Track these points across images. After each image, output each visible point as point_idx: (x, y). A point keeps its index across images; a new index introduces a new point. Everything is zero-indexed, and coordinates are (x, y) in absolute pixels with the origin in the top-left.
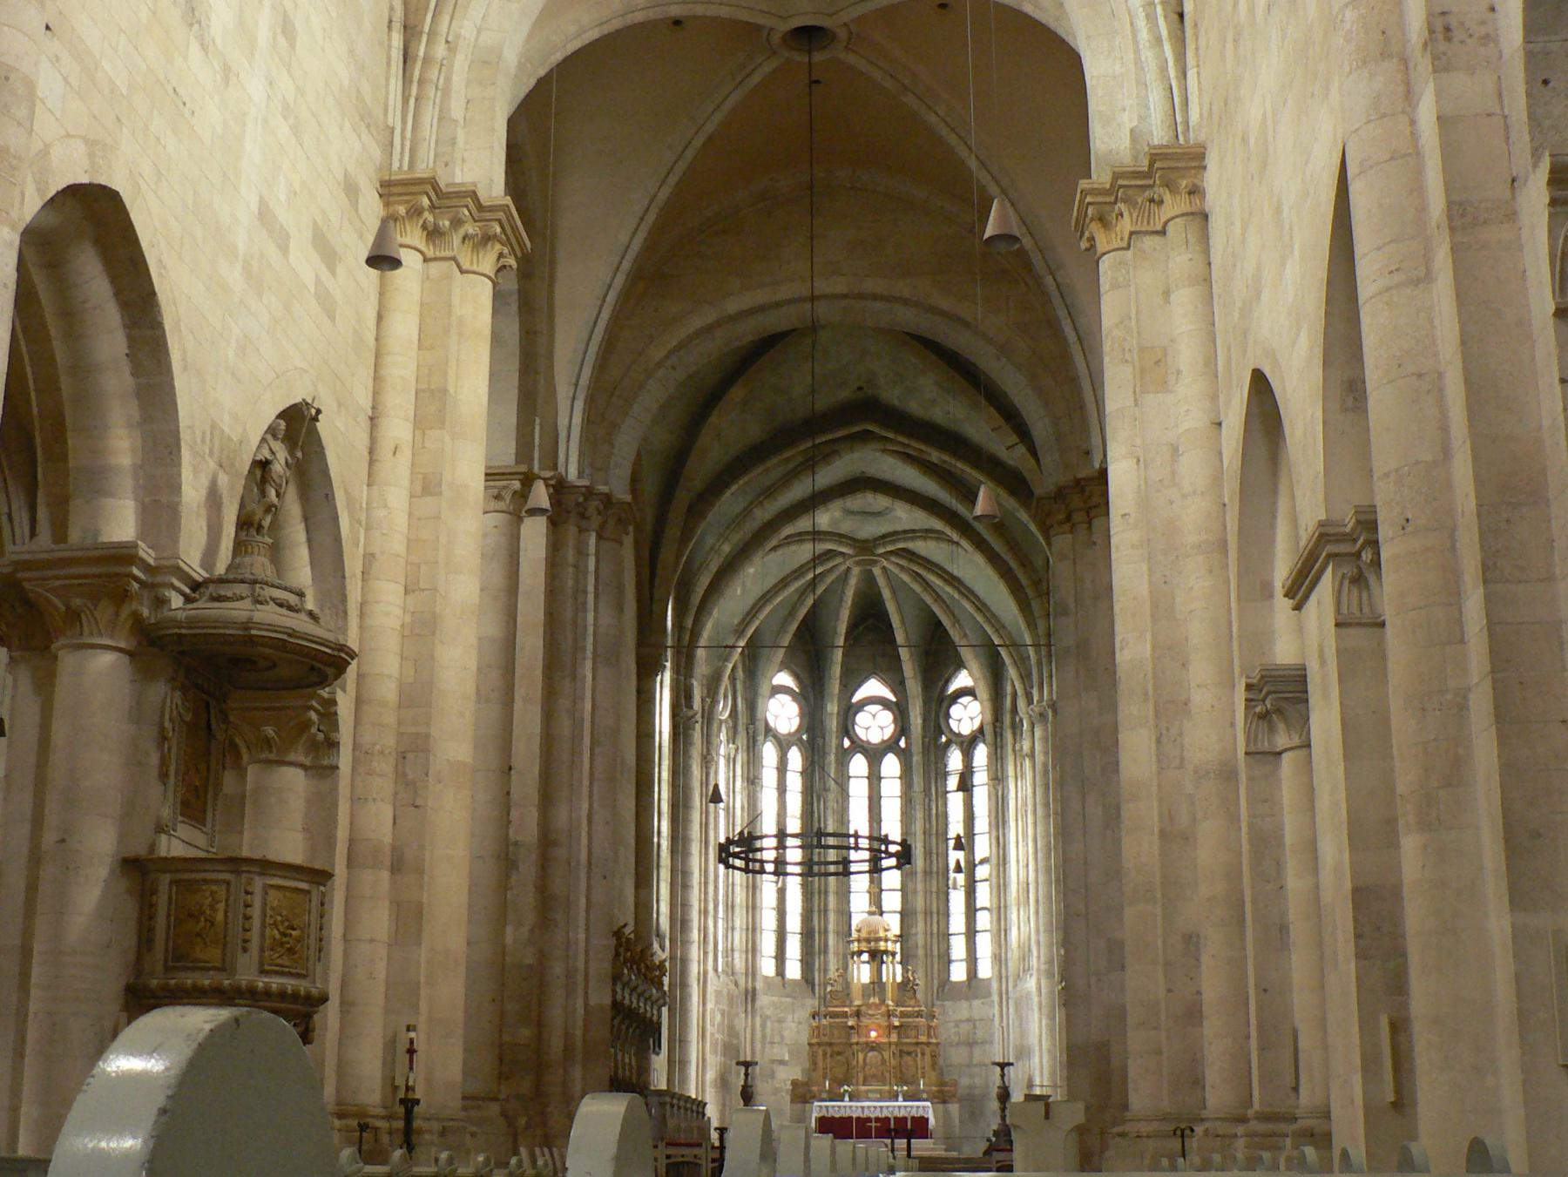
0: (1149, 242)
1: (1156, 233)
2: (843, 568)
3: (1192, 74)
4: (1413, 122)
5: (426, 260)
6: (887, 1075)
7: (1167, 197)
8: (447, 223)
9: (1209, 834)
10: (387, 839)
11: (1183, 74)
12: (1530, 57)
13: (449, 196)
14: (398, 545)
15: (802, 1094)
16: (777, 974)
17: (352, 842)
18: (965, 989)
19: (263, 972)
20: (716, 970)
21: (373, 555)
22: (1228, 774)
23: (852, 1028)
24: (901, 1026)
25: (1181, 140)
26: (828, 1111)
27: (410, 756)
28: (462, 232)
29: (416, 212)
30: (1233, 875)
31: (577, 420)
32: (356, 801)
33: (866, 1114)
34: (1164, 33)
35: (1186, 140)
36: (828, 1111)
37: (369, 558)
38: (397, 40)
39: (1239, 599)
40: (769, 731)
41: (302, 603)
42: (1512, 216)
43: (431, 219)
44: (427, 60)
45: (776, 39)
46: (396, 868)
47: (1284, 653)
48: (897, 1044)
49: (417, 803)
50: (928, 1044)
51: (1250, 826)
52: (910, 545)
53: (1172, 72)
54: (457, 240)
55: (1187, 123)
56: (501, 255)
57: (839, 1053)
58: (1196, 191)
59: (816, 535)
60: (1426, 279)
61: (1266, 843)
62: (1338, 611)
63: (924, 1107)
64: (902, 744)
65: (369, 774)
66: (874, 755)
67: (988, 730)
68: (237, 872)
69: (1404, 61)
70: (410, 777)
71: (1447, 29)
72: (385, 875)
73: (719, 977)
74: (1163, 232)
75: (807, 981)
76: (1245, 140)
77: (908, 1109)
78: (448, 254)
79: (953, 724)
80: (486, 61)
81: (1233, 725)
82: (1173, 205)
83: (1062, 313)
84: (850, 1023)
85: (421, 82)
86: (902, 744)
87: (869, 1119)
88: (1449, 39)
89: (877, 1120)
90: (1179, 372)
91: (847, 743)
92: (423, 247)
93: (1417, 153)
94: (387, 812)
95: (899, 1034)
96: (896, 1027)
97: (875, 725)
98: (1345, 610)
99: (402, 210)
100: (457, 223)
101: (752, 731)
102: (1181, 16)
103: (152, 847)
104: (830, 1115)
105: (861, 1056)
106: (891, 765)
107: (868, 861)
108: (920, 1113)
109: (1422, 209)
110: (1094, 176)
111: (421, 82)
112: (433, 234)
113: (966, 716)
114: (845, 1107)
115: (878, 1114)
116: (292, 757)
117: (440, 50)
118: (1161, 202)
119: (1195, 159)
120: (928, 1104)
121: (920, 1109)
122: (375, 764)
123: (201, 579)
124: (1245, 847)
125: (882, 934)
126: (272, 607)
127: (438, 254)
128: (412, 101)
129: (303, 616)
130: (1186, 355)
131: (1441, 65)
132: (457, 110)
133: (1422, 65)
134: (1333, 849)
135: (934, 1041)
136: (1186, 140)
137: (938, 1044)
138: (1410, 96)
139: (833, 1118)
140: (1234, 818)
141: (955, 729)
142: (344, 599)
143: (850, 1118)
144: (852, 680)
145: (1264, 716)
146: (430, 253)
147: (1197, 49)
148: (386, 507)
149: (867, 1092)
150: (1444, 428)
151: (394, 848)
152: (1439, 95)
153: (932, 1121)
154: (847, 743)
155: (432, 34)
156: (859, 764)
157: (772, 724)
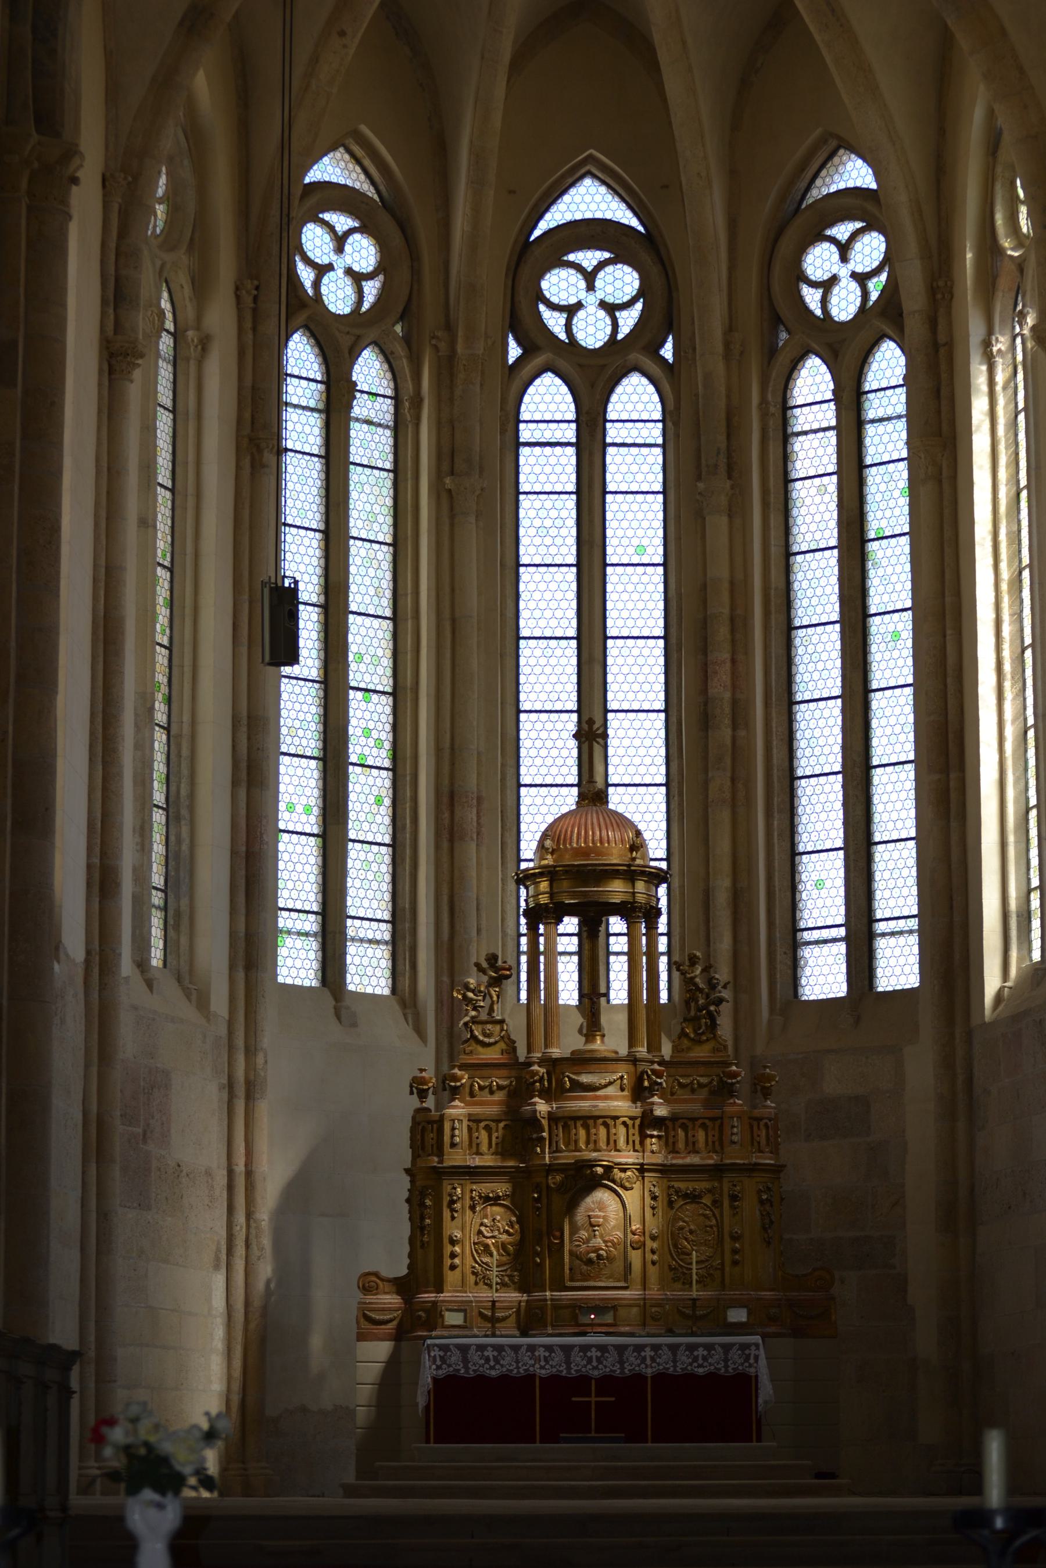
16: (324, 980)
20: (142, 963)
24: (674, 1118)
26: (465, 1361)
33: (578, 1364)
36: (465, 1361)
50: (752, 1169)
63: (744, 1347)
64: (667, 352)
67: (914, 301)
73: (150, 984)
75: (403, 1004)
77: (701, 1352)
79: (812, 298)
86: (667, 352)
87: (581, 1383)
89: (607, 1383)
91: (514, 351)
96: (659, 1123)
104: (472, 1374)
108: (736, 1363)
114: (516, 1348)
115: (610, 1365)
120: (758, 1339)
121: (735, 1355)
125: (616, 856)
137: (777, 1170)
139: (481, 1378)
143: (530, 1378)
153: (766, 1390)
154: (514, 351)
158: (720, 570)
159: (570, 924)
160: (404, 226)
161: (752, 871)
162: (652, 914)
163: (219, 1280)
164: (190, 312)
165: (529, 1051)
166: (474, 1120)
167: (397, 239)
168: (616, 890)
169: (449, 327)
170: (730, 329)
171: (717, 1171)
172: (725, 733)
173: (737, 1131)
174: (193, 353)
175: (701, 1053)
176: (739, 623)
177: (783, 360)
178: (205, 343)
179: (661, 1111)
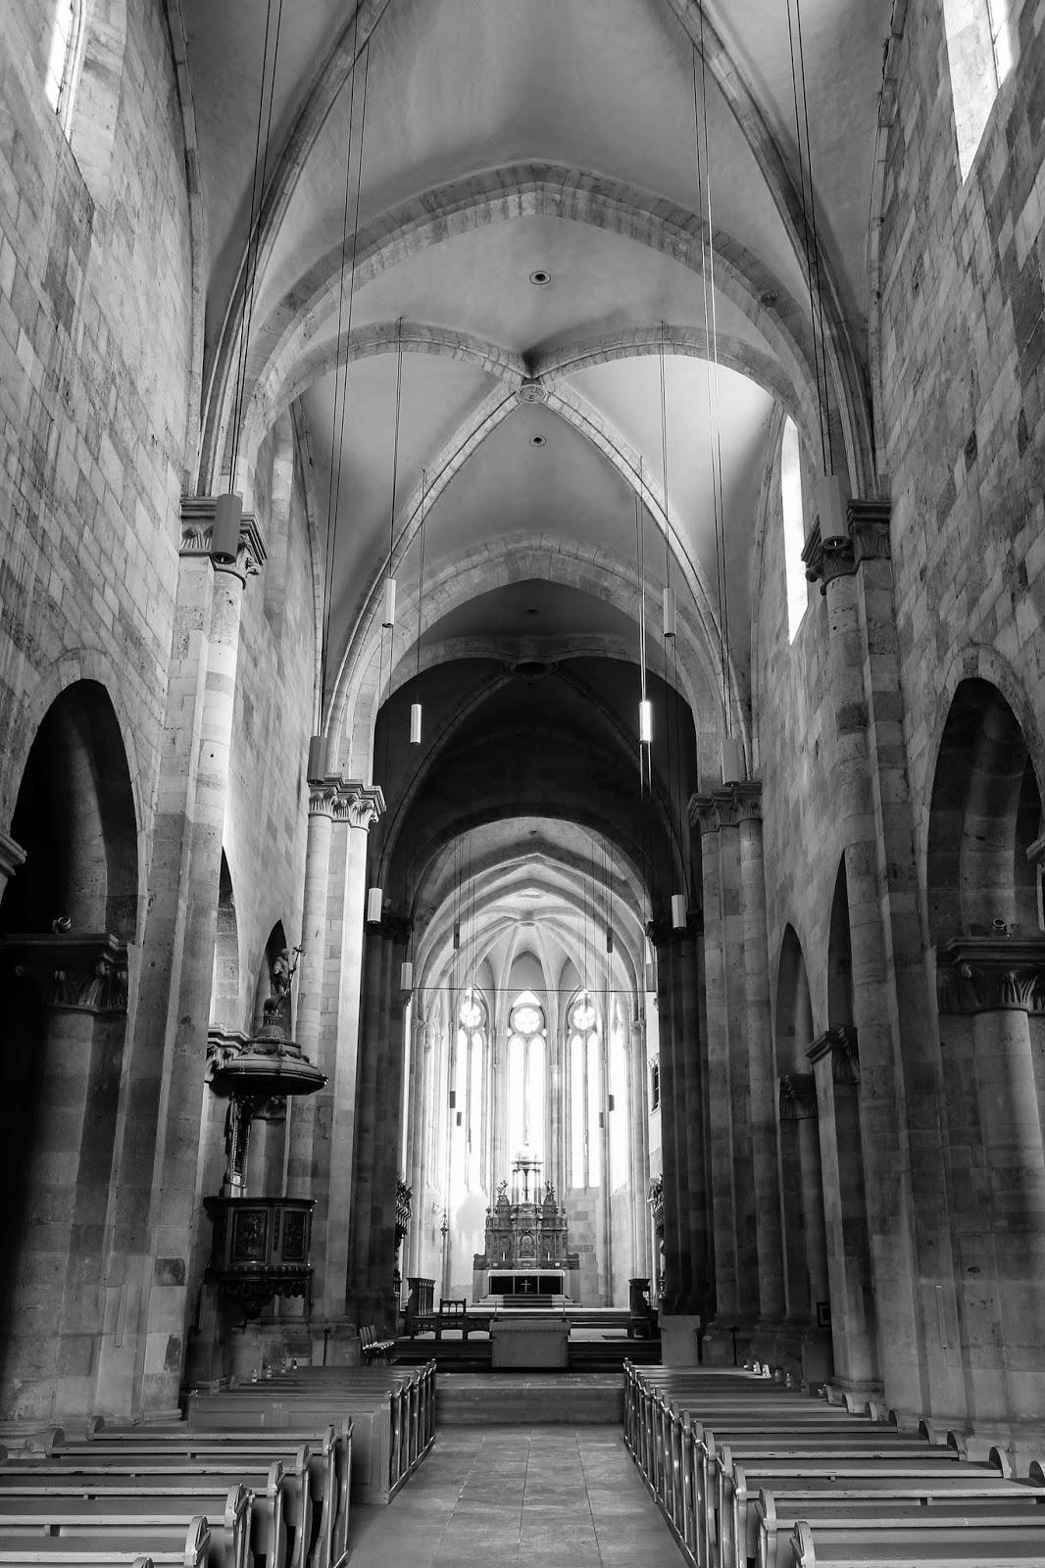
0: (729, 831)
1: (734, 826)
2: (514, 927)
3: (755, 741)
4: (879, 907)
5: (333, 822)
6: (535, 1251)
7: (741, 809)
8: (346, 802)
9: (759, 1161)
10: (310, 1159)
11: (750, 740)
12: (930, 896)
13: (346, 786)
14: (318, 988)
15: (480, 1264)
17: (290, 1161)
18: (583, 1193)
19: (284, 1260)
21: (304, 994)
22: (769, 1128)
23: (513, 1220)
25: (749, 779)
27: (322, 1109)
28: (353, 805)
29: (328, 796)
30: (773, 1183)
31: (384, 872)
32: (294, 1137)
34: (741, 716)
35: (752, 778)
37: (302, 995)
38: (318, 693)
39: (777, 1034)
40: (461, 1025)
41: (300, 1052)
42: (921, 961)
43: (337, 799)
44: (336, 707)
45: (513, 667)
46: (314, 1174)
47: (801, 1065)
48: (542, 1231)
49: (327, 1136)
50: (561, 1230)
51: (783, 1161)
52: (556, 916)
53: (744, 739)
54: (350, 810)
55: (751, 767)
56: (372, 816)
57: (505, 1237)
58: (756, 806)
59: (499, 909)
60: (883, 981)
61: (792, 1168)
62: (834, 1077)
65: (301, 1121)
66: (527, 1039)
68: (273, 1206)
69: (876, 878)
70: (322, 1121)
71: (895, 872)
72: (308, 1179)
74: (737, 826)
76: (786, 801)
78: (345, 818)
80: (364, 703)
81: (773, 1101)
82: (742, 815)
83: (665, 822)
84: (512, 1217)
85: (332, 719)
88: (895, 877)
90: (745, 906)
92: (331, 814)
93: (881, 922)
94: (310, 1142)
95: (542, 1224)
97: (527, 1020)
98: (838, 1076)
99: (321, 795)
100: (350, 802)
101: (455, 1024)
102: (750, 706)
103: (222, 1191)
105: (519, 1239)
106: (538, 1045)
107: (587, 1187)
109: (883, 953)
110: (700, 790)
111: (332, 719)
112: (337, 807)
113: (583, 1018)
116: (261, 1114)
117: (343, 701)
118: (736, 810)
119: (757, 788)
122: (304, 1116)
123: (246, 1040)
124: (780, 1170)
126: (288, 1058)
127: (340, 819)
128: (327, 730)
129: (302, 1061)
130: (748, 897)
131: (892, 889)
132: (349, 734)
133: (884, 885)
134: (832, 1194)
135: (565, 1228)
136: (752, 778)
138: (878, 894)
140: (774, 1153)
141: (578, 1026)
142: (290, 1022)
144: (514, 990)
145: (790, 1100)
146: (335, 818)
147: (758, 728)
148: (311, 966)
149: (523, 1262)
150: (891, 1050)
151: (313, 1163)
152: (891, 901)
155: (339, 692)
156: (516, 1045)
157: (463, 1021)
158: (555, 1086)
159: (522, 1172)
160: (485, 1004)
161: (562, 1157)
162: (539, 1171)
163: (442, 1255)
164: (439, 1031)
165: (513, 1202)
166: (500, 1219)
167: (483, 1007)
168: (532, 1166)
169: (495, 1029)
170: (558, 1030)
171: (554, 1231)
172: (555, 1125)
173: (558, 1222)
174: (439, 1040)
175: (550, 1203)
176: (559, 1100)
177: (570, 1037)
178: (442, 1038)
179: (541, 1217)
